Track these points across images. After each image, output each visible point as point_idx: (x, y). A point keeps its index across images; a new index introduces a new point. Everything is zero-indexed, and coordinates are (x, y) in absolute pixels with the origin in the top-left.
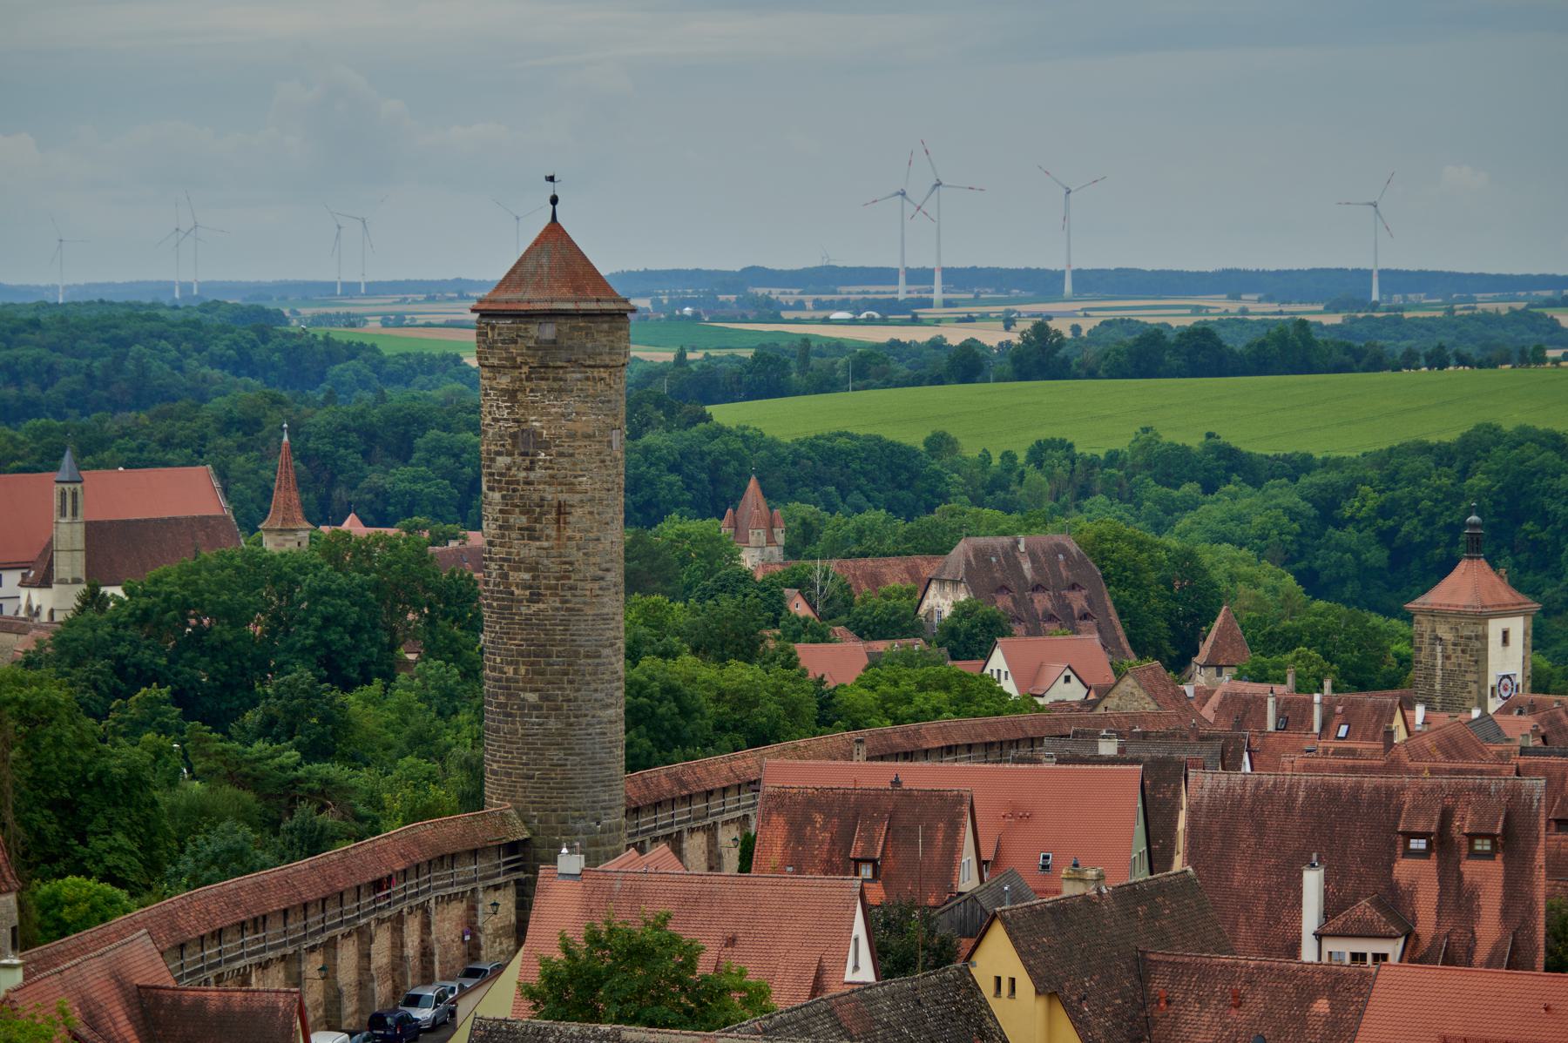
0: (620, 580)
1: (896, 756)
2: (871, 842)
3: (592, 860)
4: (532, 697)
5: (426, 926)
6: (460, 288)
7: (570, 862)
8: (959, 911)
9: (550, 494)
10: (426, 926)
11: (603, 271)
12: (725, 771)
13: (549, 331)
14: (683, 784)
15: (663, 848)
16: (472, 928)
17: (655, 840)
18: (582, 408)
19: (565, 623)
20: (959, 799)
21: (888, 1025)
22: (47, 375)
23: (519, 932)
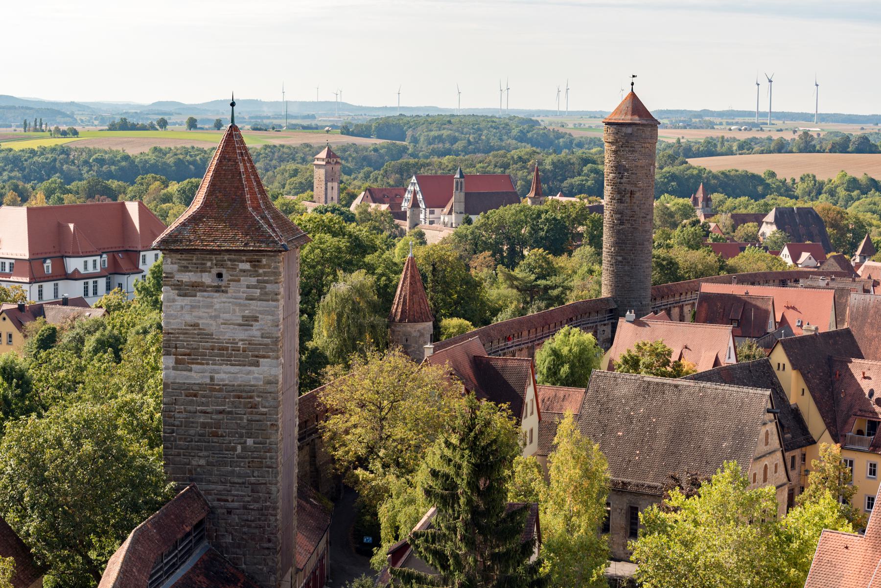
3: (638, 316)
4: (620, 258)
6: (601, 114)
9: (629, 188)
18: (641, 157)
21: (739, 379)
22: (454, 140)
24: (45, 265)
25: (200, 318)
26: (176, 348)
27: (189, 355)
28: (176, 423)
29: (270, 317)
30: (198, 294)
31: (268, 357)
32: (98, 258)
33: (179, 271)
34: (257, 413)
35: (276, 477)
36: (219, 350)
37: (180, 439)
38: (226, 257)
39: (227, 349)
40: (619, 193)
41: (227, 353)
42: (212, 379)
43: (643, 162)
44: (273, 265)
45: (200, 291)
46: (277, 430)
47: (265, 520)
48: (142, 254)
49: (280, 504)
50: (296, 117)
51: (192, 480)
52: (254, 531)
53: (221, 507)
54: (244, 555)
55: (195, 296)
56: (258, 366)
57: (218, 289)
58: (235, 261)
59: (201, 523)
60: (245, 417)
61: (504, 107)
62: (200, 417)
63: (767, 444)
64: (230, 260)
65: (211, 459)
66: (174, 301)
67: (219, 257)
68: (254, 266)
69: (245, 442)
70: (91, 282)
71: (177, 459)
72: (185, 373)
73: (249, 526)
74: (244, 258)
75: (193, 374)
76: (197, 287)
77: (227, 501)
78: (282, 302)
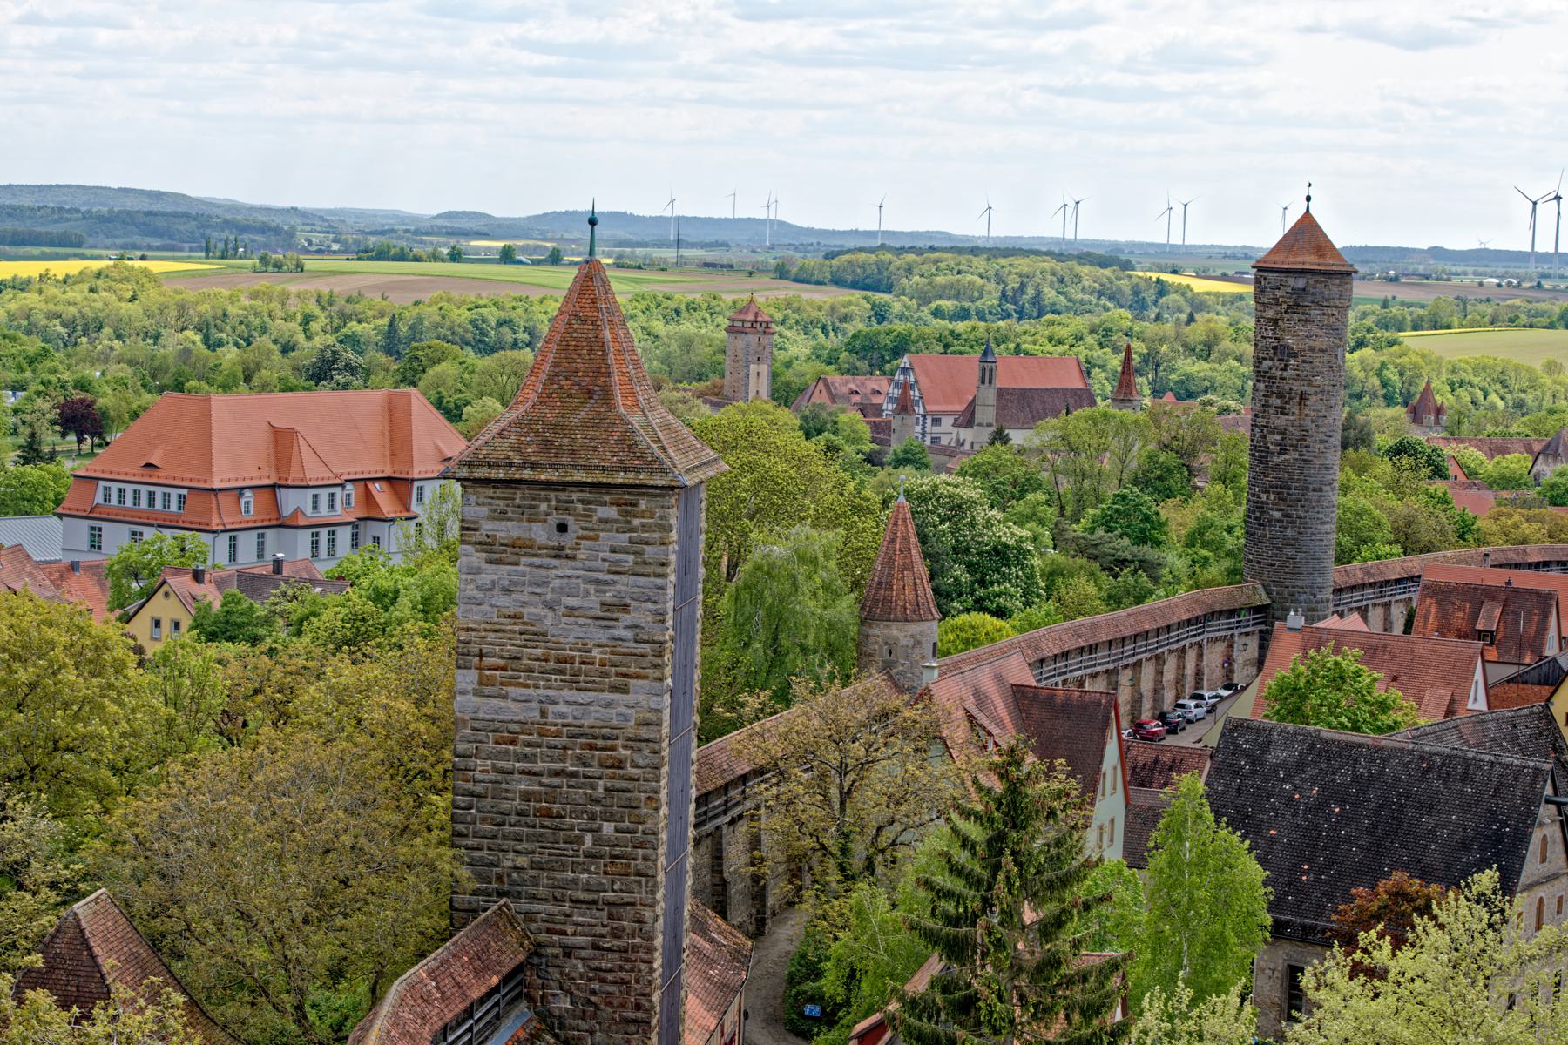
0: (1338, 443)
1: (1509, 566)
2: (1489, 618)
4: (1277, 515)
5: (1200, 656)
6: (1244, 253)
7: (1295, 619)
8: (1545, 669)
9: (1297, 387)
10: (1200, 656)
11: (1338, 245)
12: (1398, 569)
13: (1301, 283)
14: (1368, 574)
15: (1356, 615)
16: (1229, 659)
17: (1351, 610)
18: (1320, 332)
19: (1301, 468)
20: (1549, 596)
21: (1493, 739)
23: (1260, 663)
24: (243, 501)
25: (524, 604)
26: (481, 655)
27: (504, 669)
28: (479, 789)
29: (650, 606)
30: (524, 560)
31: (645, 677)
32: (338, 491)
33: (490, 518)
34: (623, 778)
35: (653, 893)
36: (559, 661)
37: (483, 821)
38: (575, 496)
39: (571, 661)
40: (1281, 397)
41: (568, 668)
42: (543, 714)
43: (1322, 342)
44: (658, 512)
45: (526, 554)
46: (657, 810)
47: (632, 970)
48: (416, 484)
49: (659, 941)
50: (693, 245)
51: (501, 894)
52: (610, 988)
53: (553, 945)
54: (592, 1033)
55: (517, 564)
56: (626, 692)
57: (558, 553)
58: (590, 503)
59: (518, 969)
60: (601, 782)
61: (1070, 235)
62: (519, 782)
63: (1543, 860)
64: (582, 501)
65: (537, 857)
66: (478, 571)
67: (563, 496)
68: (626, 514)
69: (599, 829)
70: (324, 532)
71: (477, 854)
72: (495, 701)
73: (603, 981)
74: (607, 498)
75: (510, 704)
76: (521, 547)
77: (564, 933)
78: (673, 578)
